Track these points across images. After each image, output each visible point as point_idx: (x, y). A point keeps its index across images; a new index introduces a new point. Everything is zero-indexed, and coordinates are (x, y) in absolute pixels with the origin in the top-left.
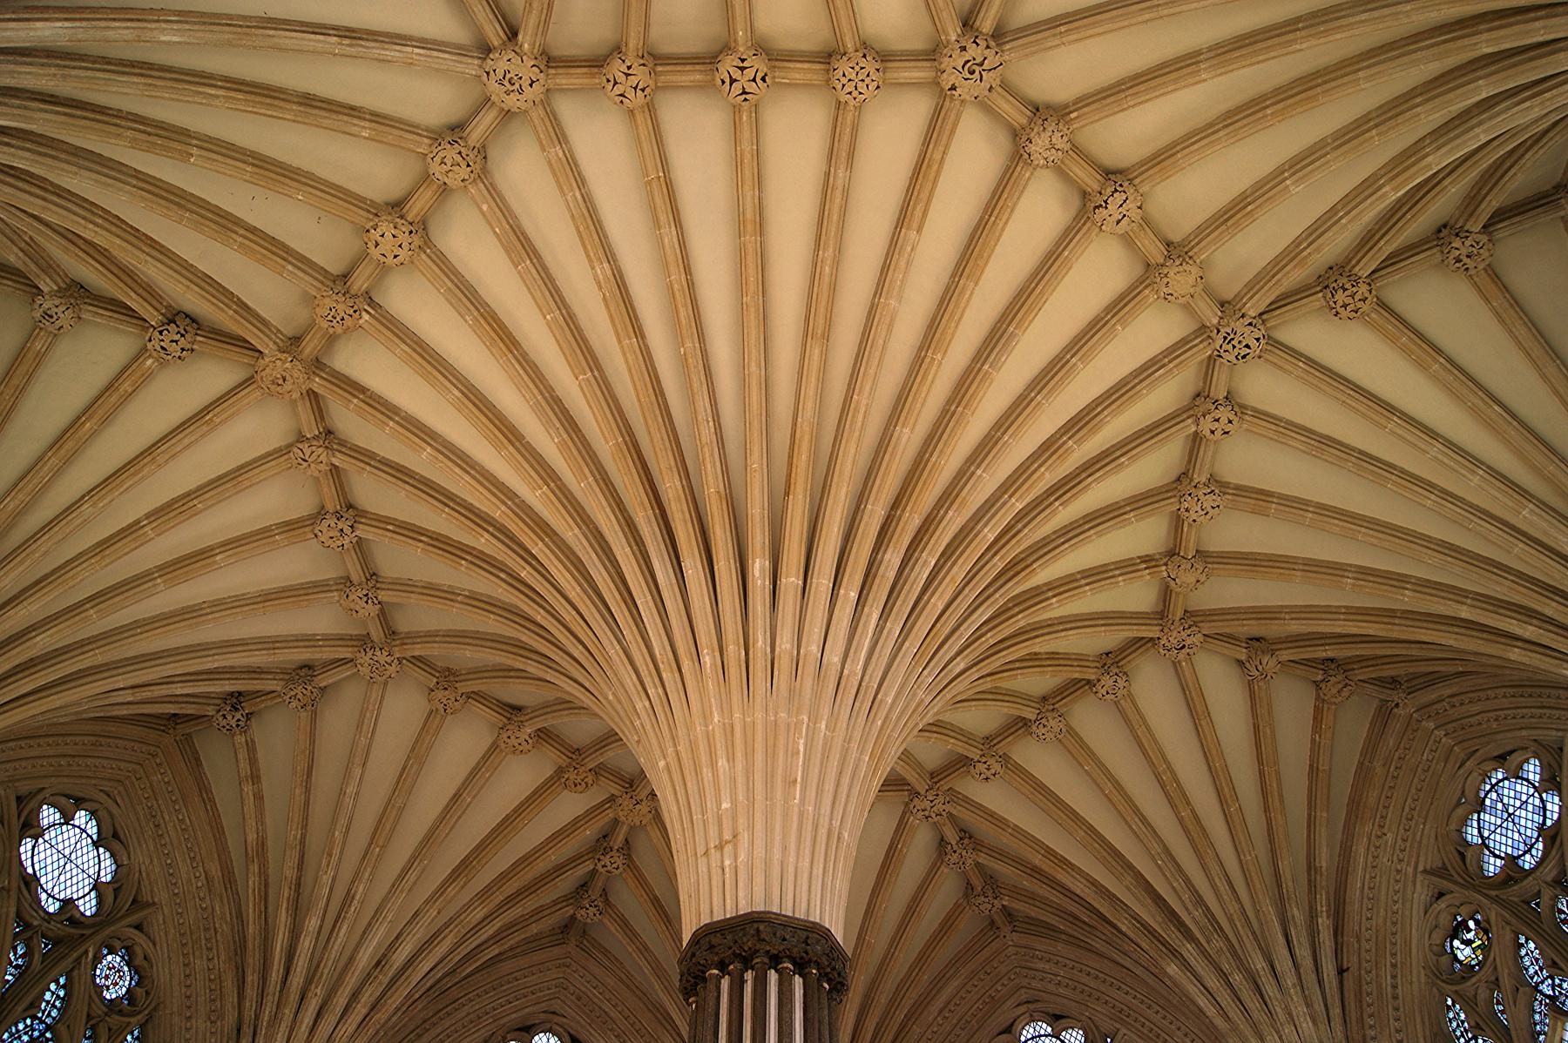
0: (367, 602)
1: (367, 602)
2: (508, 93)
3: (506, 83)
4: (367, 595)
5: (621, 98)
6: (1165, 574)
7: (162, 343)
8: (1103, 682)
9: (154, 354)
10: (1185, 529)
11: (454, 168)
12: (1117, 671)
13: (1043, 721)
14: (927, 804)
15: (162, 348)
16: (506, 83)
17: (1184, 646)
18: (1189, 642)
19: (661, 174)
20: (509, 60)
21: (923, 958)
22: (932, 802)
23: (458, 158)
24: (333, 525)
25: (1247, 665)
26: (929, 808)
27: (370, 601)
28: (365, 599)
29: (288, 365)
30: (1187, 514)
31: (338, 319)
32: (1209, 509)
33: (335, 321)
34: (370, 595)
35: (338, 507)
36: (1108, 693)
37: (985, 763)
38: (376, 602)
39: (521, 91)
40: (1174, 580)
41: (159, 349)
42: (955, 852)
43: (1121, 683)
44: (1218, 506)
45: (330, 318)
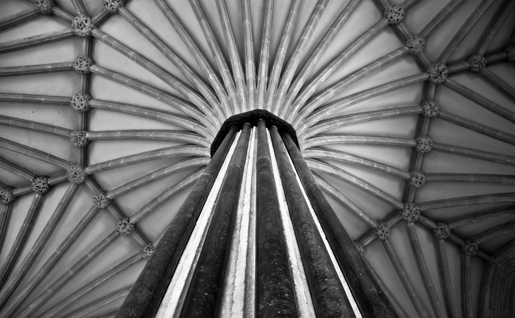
0: (150, 250)
1: (150, 250)
2: (82, 29)
3: (80, 27)
4: (148, 248)
5: (111, 7)
6: (408, 49)
7: (37, 185)
8: (426, 109)
9: (36, 191)
10: (401, 29)
11: (82, 63)
12: (427, 102)
13: (420, 142)
14: (407, 211)
15: (38, 187)
16: (80, 27)
17: (441, 73)
18: (440, 69)
19: (135, 19)
20: (76, 20)
21: (463, 288)
22: (409, 209)
23: (81, 60)
24: (121, 223)
25: (472, 66)
26: (410, 213)
27: (151, 249)
28: (148, 249)
29: (75, 168)
30: (392, 19)
31: (79, 139)
32: (399, 12)
33: (78, 141)
34: (150, 247)
35: (121, 218)
36: (432, 112)
37: (414, 176)
38: (153, 248)
39: (85, 26)
40: (412, 47)
41: (36, 188)
42: (438, 229)
43: (433, 105)
44: (400, 8)
45: (76, 141)
